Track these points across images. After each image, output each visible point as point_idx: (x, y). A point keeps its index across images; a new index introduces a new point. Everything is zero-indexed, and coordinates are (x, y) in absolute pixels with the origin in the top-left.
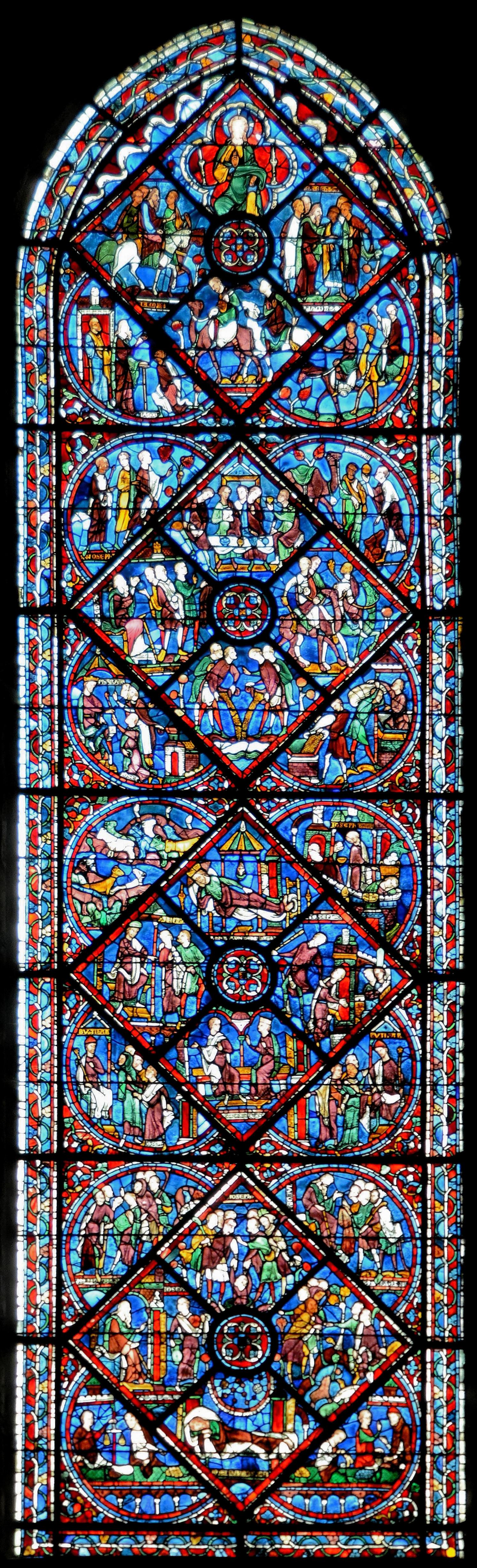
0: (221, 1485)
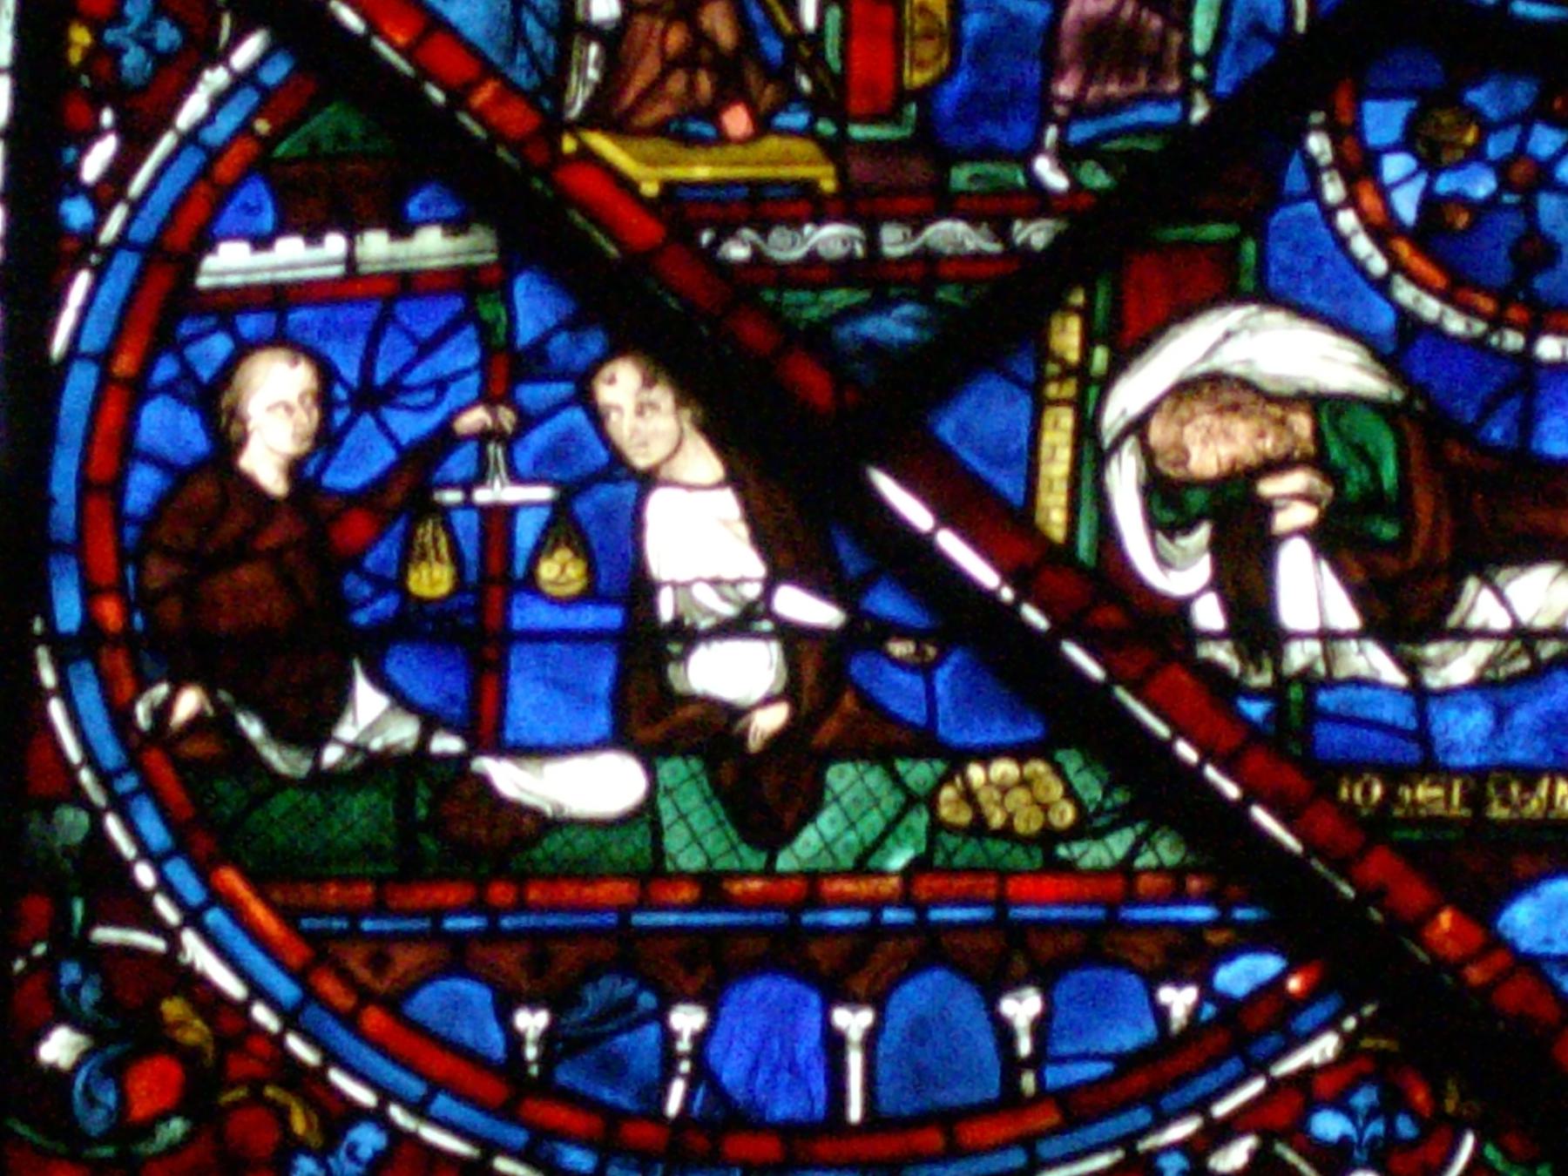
0: (1412, 894)
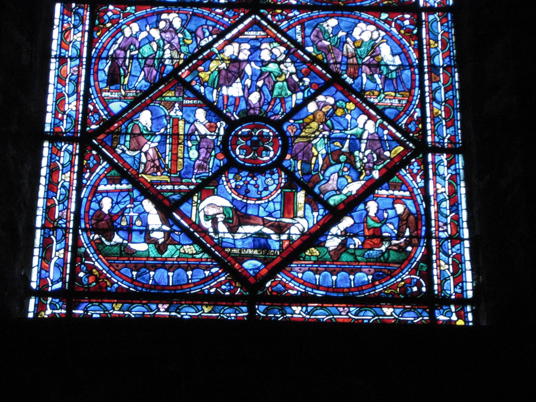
0: (233, 262)
